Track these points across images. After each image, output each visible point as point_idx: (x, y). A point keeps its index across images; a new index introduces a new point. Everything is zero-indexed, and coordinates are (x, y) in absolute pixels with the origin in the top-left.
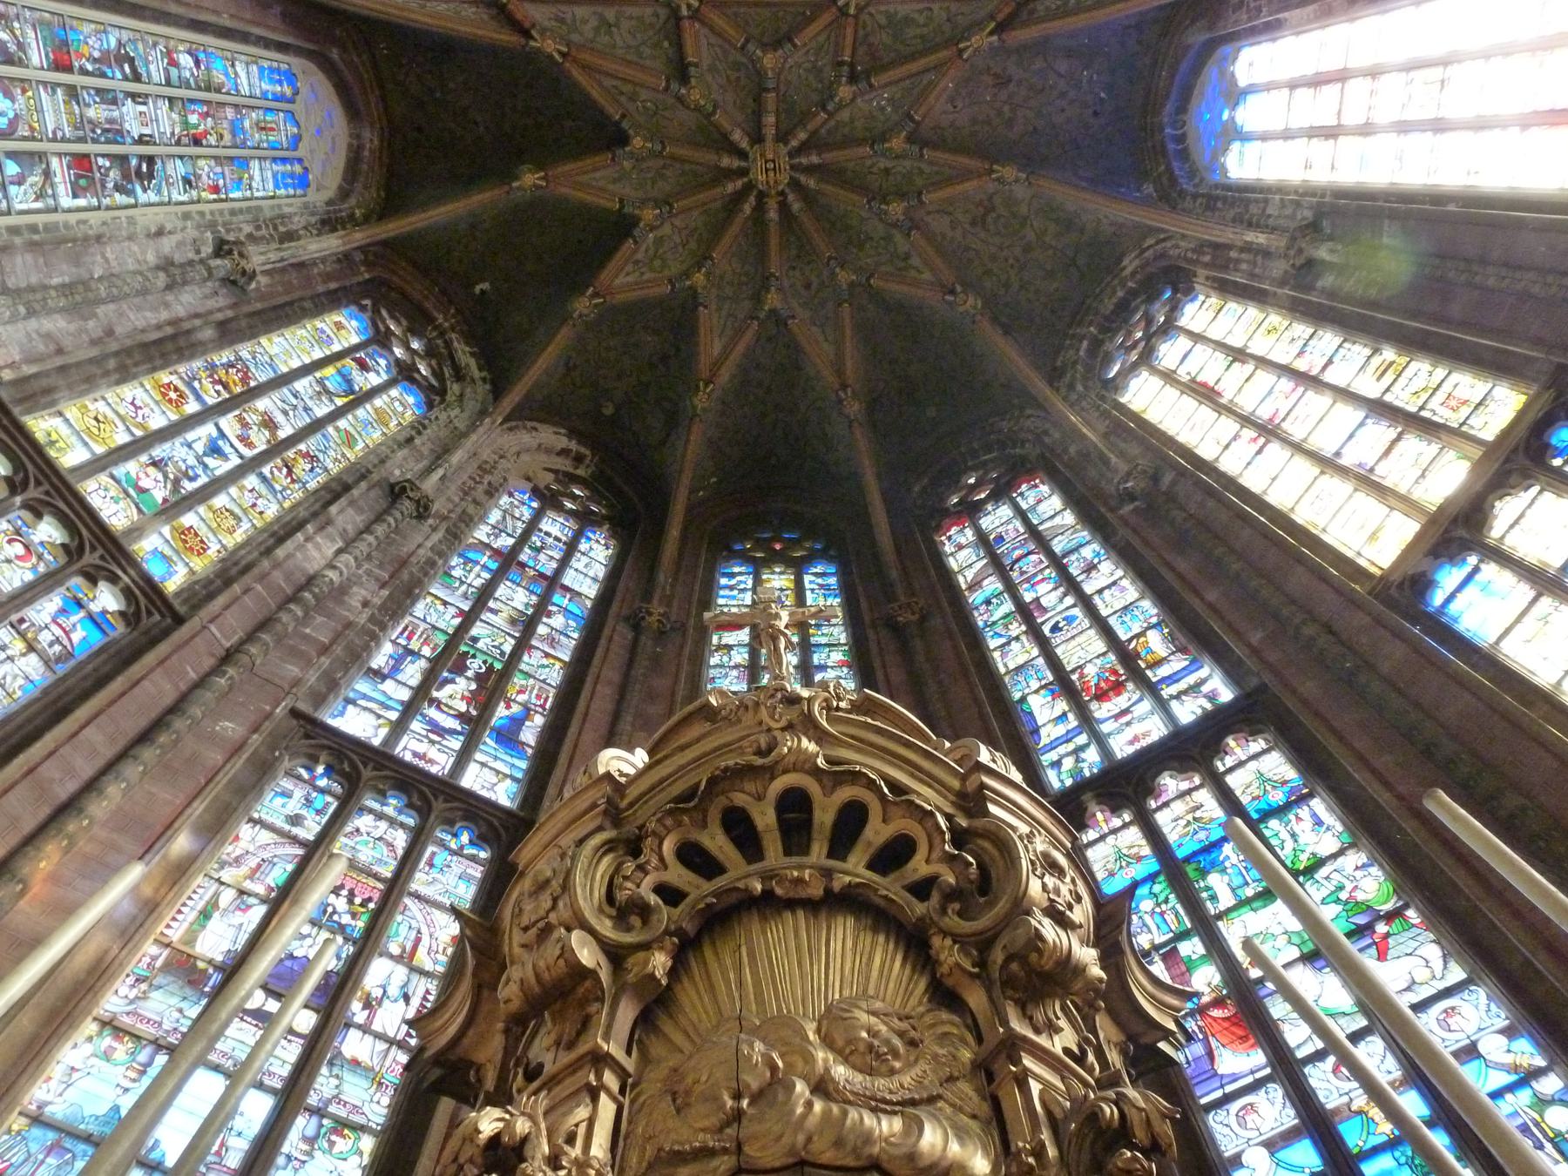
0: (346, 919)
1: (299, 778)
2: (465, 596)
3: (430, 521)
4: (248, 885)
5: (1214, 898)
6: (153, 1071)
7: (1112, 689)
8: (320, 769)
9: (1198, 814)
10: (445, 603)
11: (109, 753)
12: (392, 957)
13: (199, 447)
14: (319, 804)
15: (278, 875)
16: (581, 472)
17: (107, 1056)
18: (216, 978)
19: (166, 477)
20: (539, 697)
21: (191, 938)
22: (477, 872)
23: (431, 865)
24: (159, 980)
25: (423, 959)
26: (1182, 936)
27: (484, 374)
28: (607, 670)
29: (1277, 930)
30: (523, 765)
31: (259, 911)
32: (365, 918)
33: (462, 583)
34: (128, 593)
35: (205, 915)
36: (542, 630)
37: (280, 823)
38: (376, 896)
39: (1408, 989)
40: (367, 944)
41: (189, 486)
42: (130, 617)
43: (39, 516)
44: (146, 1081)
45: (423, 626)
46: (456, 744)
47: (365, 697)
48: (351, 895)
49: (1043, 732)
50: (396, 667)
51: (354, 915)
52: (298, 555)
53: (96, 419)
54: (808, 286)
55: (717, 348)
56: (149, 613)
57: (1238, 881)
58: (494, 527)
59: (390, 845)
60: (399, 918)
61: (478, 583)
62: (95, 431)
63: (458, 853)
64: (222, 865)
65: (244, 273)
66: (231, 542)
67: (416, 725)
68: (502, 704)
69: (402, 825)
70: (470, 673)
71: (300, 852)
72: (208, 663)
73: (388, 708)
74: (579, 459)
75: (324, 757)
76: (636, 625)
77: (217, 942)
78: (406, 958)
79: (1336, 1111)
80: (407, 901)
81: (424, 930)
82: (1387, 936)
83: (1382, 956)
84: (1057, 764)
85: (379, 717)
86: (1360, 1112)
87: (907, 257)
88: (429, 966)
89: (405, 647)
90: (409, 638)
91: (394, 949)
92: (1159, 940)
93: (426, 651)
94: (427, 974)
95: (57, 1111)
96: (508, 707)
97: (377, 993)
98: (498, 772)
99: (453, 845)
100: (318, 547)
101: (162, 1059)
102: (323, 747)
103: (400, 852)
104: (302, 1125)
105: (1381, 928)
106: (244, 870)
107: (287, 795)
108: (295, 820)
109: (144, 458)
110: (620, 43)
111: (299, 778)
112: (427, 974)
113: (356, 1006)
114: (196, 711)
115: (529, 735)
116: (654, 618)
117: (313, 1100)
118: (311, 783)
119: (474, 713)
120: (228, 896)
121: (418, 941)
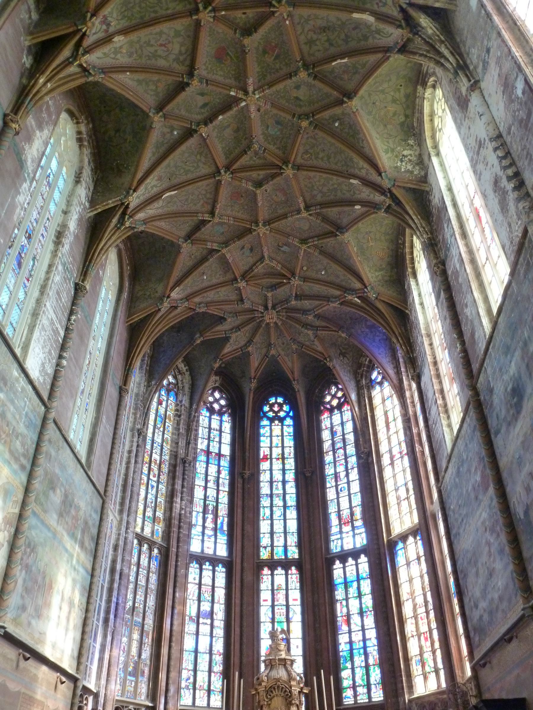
10: (200, 486)
16: (217, 385)
27: (187, 367)
28: (239, 502)
30: (226, 538)
31: (196, 602)
34: (158, 548)
36: (221, 481)
40: (213, 602)
41: (153, 505)
47: (195, 535)
50: (197, 521)
54: (283, 344)
55: (256, 364)
67: (206, 538)
70: (210, 512)
76: (243, 477)
84: (333, 541)
87: (313, 341)
104: (214, 639)
110: (221, 295)
115: (225, 528)
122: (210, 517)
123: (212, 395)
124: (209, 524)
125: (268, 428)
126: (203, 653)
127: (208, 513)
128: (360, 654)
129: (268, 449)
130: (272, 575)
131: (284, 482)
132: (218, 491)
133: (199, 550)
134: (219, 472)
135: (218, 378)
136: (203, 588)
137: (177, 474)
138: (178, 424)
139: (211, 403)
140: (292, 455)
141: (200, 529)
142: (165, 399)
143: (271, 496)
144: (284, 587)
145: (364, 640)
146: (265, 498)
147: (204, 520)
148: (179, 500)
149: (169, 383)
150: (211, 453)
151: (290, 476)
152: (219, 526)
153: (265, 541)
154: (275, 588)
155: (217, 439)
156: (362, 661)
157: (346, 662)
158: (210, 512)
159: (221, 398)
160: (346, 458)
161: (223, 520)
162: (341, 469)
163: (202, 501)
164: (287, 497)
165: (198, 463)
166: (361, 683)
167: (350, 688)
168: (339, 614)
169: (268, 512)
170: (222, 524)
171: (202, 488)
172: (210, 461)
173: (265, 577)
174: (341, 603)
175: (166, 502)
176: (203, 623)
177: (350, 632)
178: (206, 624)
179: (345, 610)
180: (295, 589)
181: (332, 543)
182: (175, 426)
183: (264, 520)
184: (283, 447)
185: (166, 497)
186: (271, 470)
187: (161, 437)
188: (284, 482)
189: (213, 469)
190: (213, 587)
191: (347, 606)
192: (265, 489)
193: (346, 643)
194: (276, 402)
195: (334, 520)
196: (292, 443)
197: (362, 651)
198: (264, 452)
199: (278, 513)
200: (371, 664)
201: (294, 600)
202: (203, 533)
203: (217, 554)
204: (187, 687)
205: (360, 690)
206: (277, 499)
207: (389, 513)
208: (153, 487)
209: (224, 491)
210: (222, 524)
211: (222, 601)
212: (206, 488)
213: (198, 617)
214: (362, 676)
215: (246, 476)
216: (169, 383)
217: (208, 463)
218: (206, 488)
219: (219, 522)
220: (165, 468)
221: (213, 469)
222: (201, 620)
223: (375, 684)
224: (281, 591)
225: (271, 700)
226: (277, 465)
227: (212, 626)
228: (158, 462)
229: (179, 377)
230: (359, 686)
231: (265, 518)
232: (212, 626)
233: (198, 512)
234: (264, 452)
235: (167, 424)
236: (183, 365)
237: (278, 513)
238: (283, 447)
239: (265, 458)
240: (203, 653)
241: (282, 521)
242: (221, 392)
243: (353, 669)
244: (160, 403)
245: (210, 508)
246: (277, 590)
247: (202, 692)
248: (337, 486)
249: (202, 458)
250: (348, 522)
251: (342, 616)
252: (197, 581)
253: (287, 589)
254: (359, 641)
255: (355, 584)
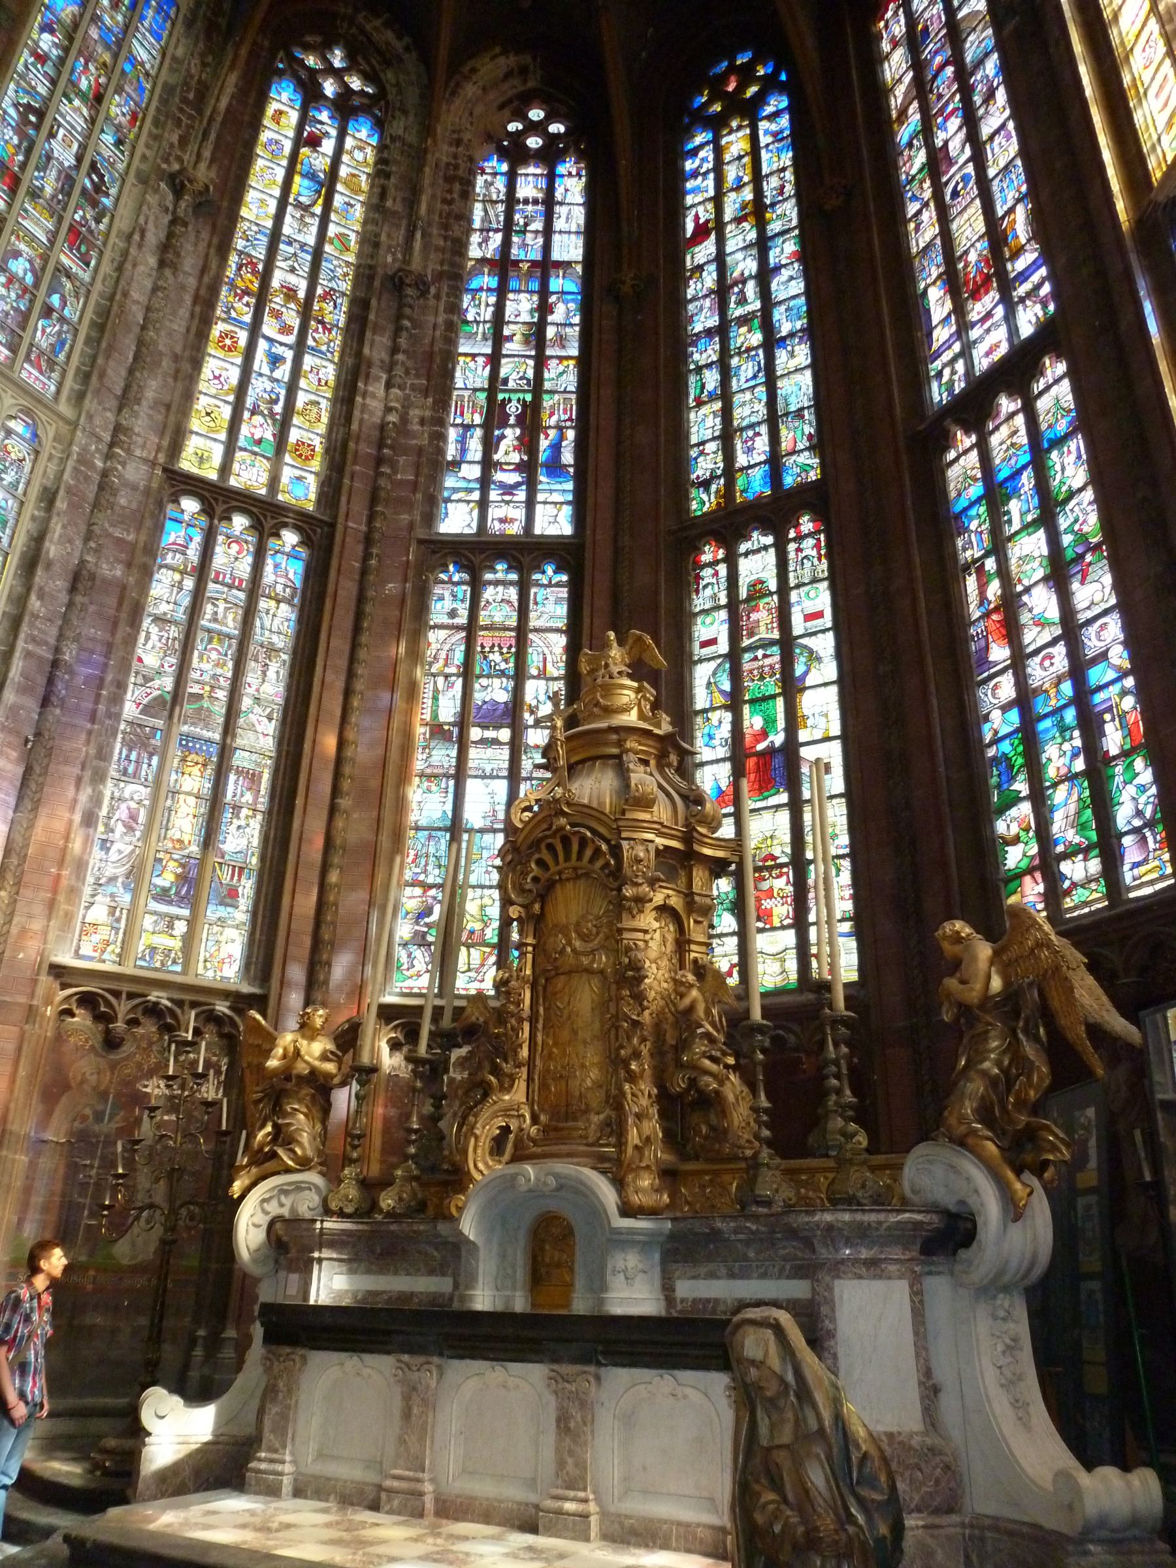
0: (503, 666)
1: (443, 582)
2: (485, 339)
3: (433, 290)
4: (447, 670)
5: (1010, 522)
6: (451, 789)
7: (982, 285)
8: (451, 568)
9: (1014, 440)
10: (474, 356)
11: (347, 648)
12: (534, 677)
13: (266, 370)
14: (460, 596)
15: (459, 656)
16: (531, 84)
17: (429, 790)
18: (456, 731)
19: (264, 416)
20: (565, 412)
21: (435, 715)
22: (564, 593)
23: (536, 603)
24: (432, 744)
25: (552, 671)
26: (986, 555)
27: (407, 40)
29: (1036, 554)
30: (570, 486)
31: (459, 683)
32: (512, 660)
33: (478, 323)
34: (297, 528)
35: (435, 699)
36: (551, 332)
37: (446, 620)
38: (513, 642)
39: (1088, 608)
41: (278, 408)
42: (306, 541)
43: (230, 519)
44: (451, 796)
45: (466, 394)
46: (521, 495)
47: (455, 490)
48: (501, 648)
49: (935, 334)
50: (463, 450)
51: (506, 661)
52: (366, 416)
53: (208, 414)
56: (315, 532)
57: (1025, 508)
58: (481, 230)
59: (509, 602)
60: (530, 650)
61: (488, 317)
62: (212, 424)
63: (550, 585)
64: (431, 664)
65: (200, 193)
66: (322, 428)
67: (494, 495)
68: (542, 436)
69: (511, 583)
70: (512, 420)
71: (464, 634)
72: (360, 548)
73: (470, 491)
74: (523, 71)
75: (449, 559)
77: (448, 710)
78: (542, 675)
79: (1035, 690)
80: (531, 636)
81: (547, 651)
82: (1090, 564)
83: (1082, 583)
85: (468, 502)
86: (1046, 691)
88: (556, 674)
89: (462, 425)
90: (462, 414)
91: (534, 672)
92: (977, 555)
93: (478, 419)
94: (556, 679)
95: (423, 822)
96: (547, 436)
97: (534, 703)
98: (555, 503)
99: (545, 582)
100: (374, 396)
101: (452, 783)
102: (445, 555)
103: (516, 604)
105: (1089, 558)
106: (442, 662)
107: (442, 598)
108: (453, 614)
109: (246, 415)
111: (443, 582)
112: (556, 679)
113: (526, 715)
114: (371, 593)
115: (568, 457)
116: (629, 282)
117: (524, 774)
118: (450, 581)
119: (525, 458)
120: (440, 680)
121: (545, 660)
122: (511, 435)
123: (522, 116)
124: (508, 450)
125: (707, 153)
126: (482, 831)
127: (504, 424)
128: (1063, 729)
129: (710, 206)
130: (731, 561)
131: (765, 275)
132: (541, 362)
133: (473, 529)
134: (544, 309)
135: (527, 59)
136: (484, 639)
137: (372, 317)
138: (383, 195)
139: (519, 136)
140: (789, 189)
141: (472, 472)
142: (333, 132)
143: (722, 331)
144: (773, 585)
145: (1078, 668)
146: (701, 345)
147: (490, 445)
148: (378, 389)
149: (346, 93)
150: (516, 263)
151: (785, 250)
152: (543, 457)
153: (706, 463)
154: (743, 593)
155: (538, 225)
156: (1075, 756)
157: (1012, 779)
158: (512, 420)
159: (549, 118)
160: (963, 76)
161: (562, 437)
162: (951, 133)
163: (482, 396)
164: (778, 314)
165: (467, 299)
166: (1072, 836)
167: (1030, 871)
168: (975, 613)
169: (712, 379)
170: (556, 448)
171: (481, 360)
172: (513, 284)
173: (707, 573)
174: (980, 571)
175: (334, 401)
176: (483, 742)
177: (1018, 661)
178: (495, 742)
179: (994, 589)
180: (815, 580)
181: (935, 386)
182: (375, 201)
183: (700, 403)
184: (758, 178)
185: (336, 389)
186: (720, 259)
187: (314, 230)
188: (765, 275)
189: (521, 307)
190: (522, 631)
191: (1003, 573)
192: (704, 318)
193: (1005, 708)
194: (732, 69)
195: (938, 303)
196: (787, 158)
197: (1070, 715)
198: (697, 217)
199: (745, 370)
200: (1114, 751)
201: (809, 617)
202: (485, 482)
203: (538, 531)
204: (420, 940)
205: (1073, 869)
206: (744, 330)
207: (1138, 117)
208: (275, 361)
209: (561, 359)
210: (556, 448)
211: (557, 669)
212: (494, 360)
213: (462, 723)
214: (1078, 813)
215: (626, 289)
216: (346, 93)
217: (502, 292)
218: (494, 360)
219: (544, 443)
220: (337, 314)
221: (521, 307)
222: (475, 733)
223: (1136, 831)
224: (762, 603)
225: (543, 898)
226: (739, 238)
227: (516, 747)
228: (301, 294)
229: (389, 76)
230: (1065, 856)
231: (704, 397)
232: (516, 747)
233: (467, 427)
234: (697, 217)
235: (338, 201)
236: (390, 35)
237: (745, 370)
238: (758, 178)
239: (702, 232)
240: (482, 831)
241: (761, 392)
242: (543, 99)
243: (1039, 797)
244: (307, 140)
245: (513, 409)
246: (747, 600)
247: (476, 954)
248: (938, 195)
249: (489, 280)
250: (987, 279)
251: (987, 615)
252: (462, 619)
253: (784, 589)
254: (1059, 680)
255: (1027, 481)
